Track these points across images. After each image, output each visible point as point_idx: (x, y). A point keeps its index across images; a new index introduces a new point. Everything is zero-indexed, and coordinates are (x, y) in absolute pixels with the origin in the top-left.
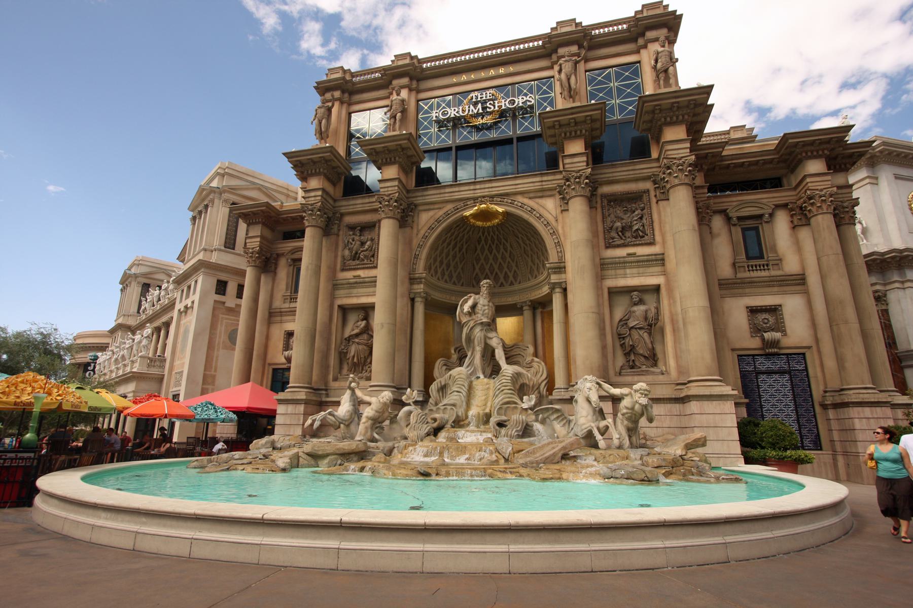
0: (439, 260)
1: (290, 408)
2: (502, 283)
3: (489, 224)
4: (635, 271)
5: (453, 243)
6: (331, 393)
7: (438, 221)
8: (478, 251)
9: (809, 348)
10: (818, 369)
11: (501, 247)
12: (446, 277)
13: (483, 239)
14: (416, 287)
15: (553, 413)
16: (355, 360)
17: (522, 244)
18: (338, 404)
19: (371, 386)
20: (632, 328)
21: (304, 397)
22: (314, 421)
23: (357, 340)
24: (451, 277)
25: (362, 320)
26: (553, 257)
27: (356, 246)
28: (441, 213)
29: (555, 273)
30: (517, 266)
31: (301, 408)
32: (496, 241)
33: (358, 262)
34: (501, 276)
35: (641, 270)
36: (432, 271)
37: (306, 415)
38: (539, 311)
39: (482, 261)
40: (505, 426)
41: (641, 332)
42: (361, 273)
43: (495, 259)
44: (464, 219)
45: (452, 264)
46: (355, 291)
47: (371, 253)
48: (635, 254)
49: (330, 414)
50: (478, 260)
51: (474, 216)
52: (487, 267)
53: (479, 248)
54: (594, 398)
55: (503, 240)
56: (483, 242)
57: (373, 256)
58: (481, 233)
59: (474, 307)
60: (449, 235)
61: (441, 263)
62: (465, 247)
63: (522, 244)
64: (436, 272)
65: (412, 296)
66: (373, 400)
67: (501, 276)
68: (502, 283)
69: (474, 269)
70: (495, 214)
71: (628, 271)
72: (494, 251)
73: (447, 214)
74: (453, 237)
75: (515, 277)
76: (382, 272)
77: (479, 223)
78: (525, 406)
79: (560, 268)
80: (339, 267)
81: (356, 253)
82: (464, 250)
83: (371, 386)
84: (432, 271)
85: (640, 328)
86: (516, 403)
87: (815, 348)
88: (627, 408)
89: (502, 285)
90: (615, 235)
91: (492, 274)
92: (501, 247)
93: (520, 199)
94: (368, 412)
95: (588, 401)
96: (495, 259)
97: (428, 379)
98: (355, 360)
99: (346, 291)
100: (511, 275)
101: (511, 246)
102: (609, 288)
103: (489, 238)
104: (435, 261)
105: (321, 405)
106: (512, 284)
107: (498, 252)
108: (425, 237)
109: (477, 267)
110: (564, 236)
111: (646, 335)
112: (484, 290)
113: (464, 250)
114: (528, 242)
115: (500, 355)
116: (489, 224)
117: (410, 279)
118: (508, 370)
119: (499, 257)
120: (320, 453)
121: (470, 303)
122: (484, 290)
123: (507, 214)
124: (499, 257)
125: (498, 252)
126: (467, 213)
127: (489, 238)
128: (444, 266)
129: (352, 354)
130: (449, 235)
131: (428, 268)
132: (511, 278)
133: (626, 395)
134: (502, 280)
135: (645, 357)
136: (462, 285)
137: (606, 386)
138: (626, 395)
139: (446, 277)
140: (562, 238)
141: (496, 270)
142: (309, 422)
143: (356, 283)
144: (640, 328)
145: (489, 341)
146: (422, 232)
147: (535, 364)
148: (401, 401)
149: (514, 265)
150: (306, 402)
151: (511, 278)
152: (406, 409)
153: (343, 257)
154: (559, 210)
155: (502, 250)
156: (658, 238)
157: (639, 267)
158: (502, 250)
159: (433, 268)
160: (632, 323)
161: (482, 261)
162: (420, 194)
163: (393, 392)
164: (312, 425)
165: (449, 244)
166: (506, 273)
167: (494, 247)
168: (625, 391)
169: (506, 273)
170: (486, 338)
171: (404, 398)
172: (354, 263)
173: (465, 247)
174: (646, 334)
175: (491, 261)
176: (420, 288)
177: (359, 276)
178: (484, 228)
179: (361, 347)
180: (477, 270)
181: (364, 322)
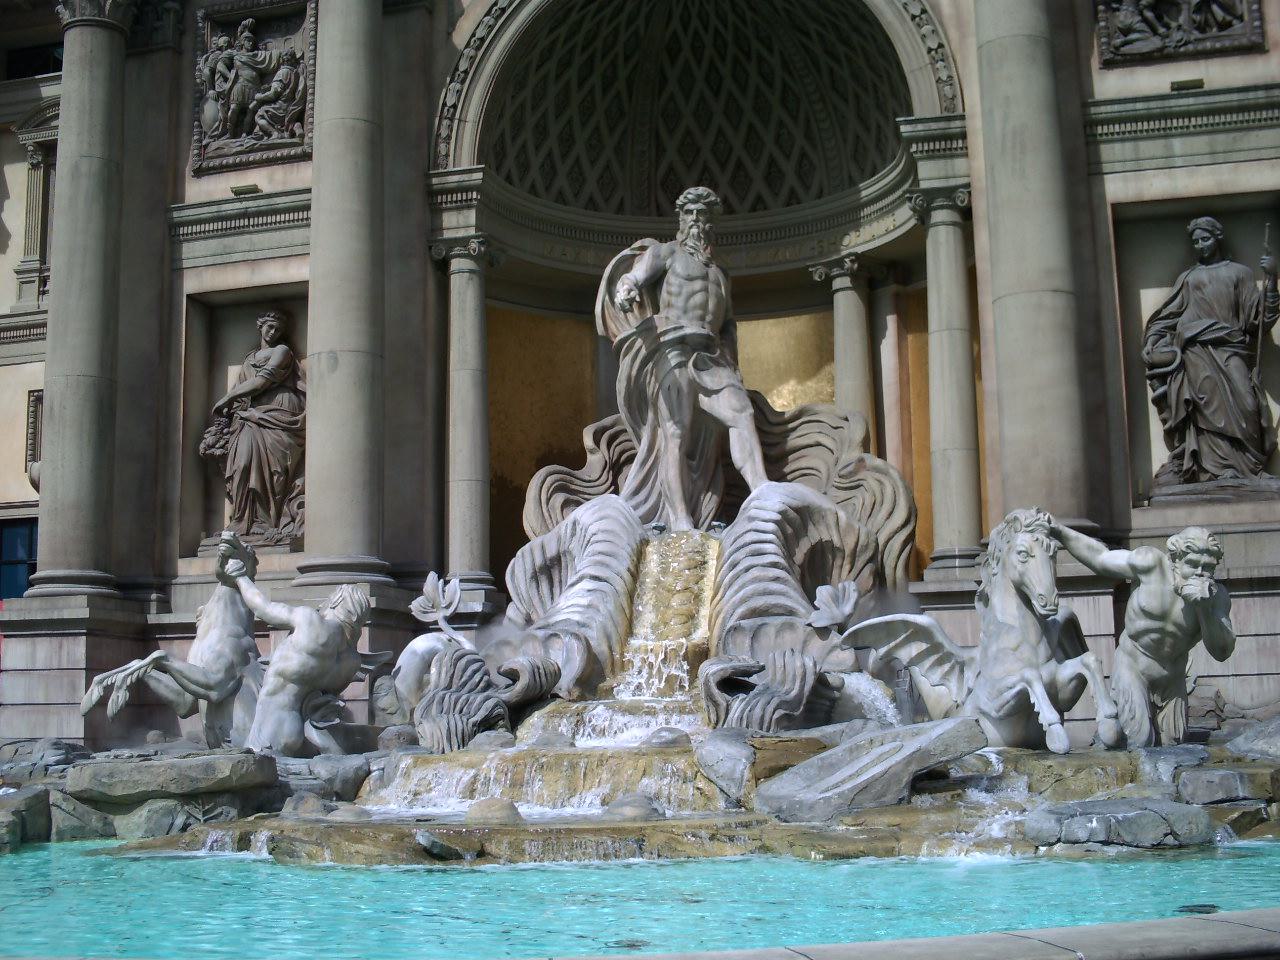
0: (531, 120)
1: (43, 650)
2: (759, 199)
4: (1200, 143)
5: (579, 59)
6: (178, 596)
12: (562, 182)
15: (908, 641)
16: (253, 482)
18: (188, 631)
19: (303, 570)
20: (1191, 342)
21: (84, 613)
22: (108, 690)
23: (255, 413)
24: (577, 177)
25: (273, 343)
26: (925, 99)
29: (932, 155)
30: (808, 136)
31: (77, 649)
33: (247, 141)
34: (757, 173)
35: (1221, 140)
36: (510, 163)
37: (93, 668)
38: (887, 292)
40: (747, 688)
41: (1220, 355)
42: (262, 179)
46: (241, 242)
47: (294, 109)
48: (1199, 84)
49: (160, 666)
54: (1040, 582)
55: (756, 45)
57: (300, 117)
58: (676, 24)
59: (653, 285)
60: (563, 30)
61: (541, 131)
62: (623, 73)
64: (525, 168)
66: (300, 616)
67: (757, 173)
68: (759, 199)
69: (660, 150)
71: (1178, 145)
74: (580, 38)
75: (803, 176)
76: (328, 174)
78: (820, 620)
79: (950, 140)
81: (243, 110)
83: (303, 570)
84: (510, 163)
86: (791, 612)
88: (1147, 614)
89: (759, 204)
90: (1134, 20)
91: (723, 166)
94: (287, 655)
97: (503, 535)
98: (253, 482)
99: (213, 245)
100: (788, 167)
102: (1114, 206)
104: (518, 126)
105: (145, 639)
106: (793, 199)
111: (1235, 367)
112: (689, 225)
114: (841, 49)
118: (767, 498)
120: (119, 792)
121: (640, 271)
122: (689, 225)
128: (552, 143)
129: (241, 462)
130: (563, 30)
131: (490, 151)
132: (791, 180)
133: (1148, 571)
134: (759, 186)
136: (620, 209)
137: (1084, 543)
138: (1148, 571)
139: (562, 182)
140: (953, 34)
142: (96, 692)
143: (245, 214)
144: (1218, 343)
145: (705, 402)
147: (870, 480)
148: (408, 616)
150: (93, 629)
151: (791, 180)
152: (421, 643)
157: (1213, 130)
159: (512, 152)
160: (1189, 326)
163: (375, 589)
164: (103, 702)
165: (565, 64)
166: (772, 162)
167: (726, 70)
169: (772, 162)
171: (416, 606)
173: (623, 73)
174: (1235, 362)
177: (252, 192)
179: (270, 437)
181: (281, 348)
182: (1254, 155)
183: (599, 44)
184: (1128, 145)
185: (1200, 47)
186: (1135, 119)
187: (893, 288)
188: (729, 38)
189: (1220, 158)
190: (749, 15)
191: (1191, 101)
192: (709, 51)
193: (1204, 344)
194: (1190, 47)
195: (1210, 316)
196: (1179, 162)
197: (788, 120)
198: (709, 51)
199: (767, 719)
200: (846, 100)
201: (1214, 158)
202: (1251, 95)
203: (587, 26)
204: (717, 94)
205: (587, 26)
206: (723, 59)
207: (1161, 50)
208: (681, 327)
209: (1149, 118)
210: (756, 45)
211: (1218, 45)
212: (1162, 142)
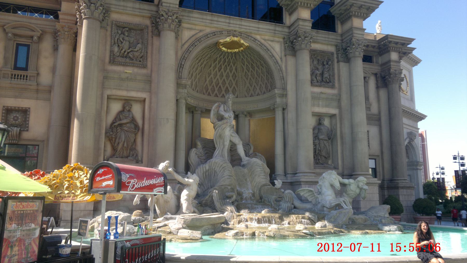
3: (229, 51)
5: (200, 58)
7: (199, 40)
8: (212, 68)
9: (378, 156)
10: (381, 168)
11: (228, 68)
13: (218, 59)
14: (181, 90)
17: (245, 70)
27: (126, 45)
28: (201, 34)
29: (279, 97)
30: (236, 84)
32: (226, 63)
38: (247, 119)
39: (212, 76)
43: (222, 76)
44: (217, 44)
45: (194, 75)
50: (210, 74)
51: (225, 45)
52: (214, 81)
53: (213, 65)
54: (337, 185)
55: (231, 64)
56: (217, 62)
58: (218, 56)
62: (205, 63)
63: (245, 70)
65: (179, 97)
69: (206, 81)
70: (241, 45)
72: (222, 70)
77: (224, 49)
79: (284, 95)
80: (107, 59)
82: (203, 65)
87: (380, 157)
95: (332, 186)
96: (222, 76)
98: (125, 145)
101: (236, 69)
103: (222, 60)
107: (225, 71)
108: (188, 51)
109: (208, 80)
110: (286, 72)
113: (203, 65)
114: (251, 69)
115: (241, 150)
116: (229, 51)
117: (177, 84)
119: (225, 75)
123: (248, 48)
124: (225, 75)
125: (225, 71)
127: (222, 60)
135: (325, 157)
140: (284, 74)
141: (220, 84)
146: (186, 46)
149: (234, 83)
153: (112, 52)
154: (283, 54)
155: (228, 70)
156: (337, 85)
158: (228, 70)
162: (186, 14)
165: (197, 59)
167: (223, 67)
168: (351, 181)
170: (231, 135)
172: (123, 60)
173: (205, 63)
175: (218, 76)
176: (184, 92)
178: (224, 51)
180: (207, 82)
187: (249, 118)
188: (227, 60)
190: (234, 57)
192: (222, 62)
197: (232, 80)
198: (222, 62)
200: (247, 79)
201: (327, 106)
204: (219, 71)
206: (223, 64)
210: (231, 64)
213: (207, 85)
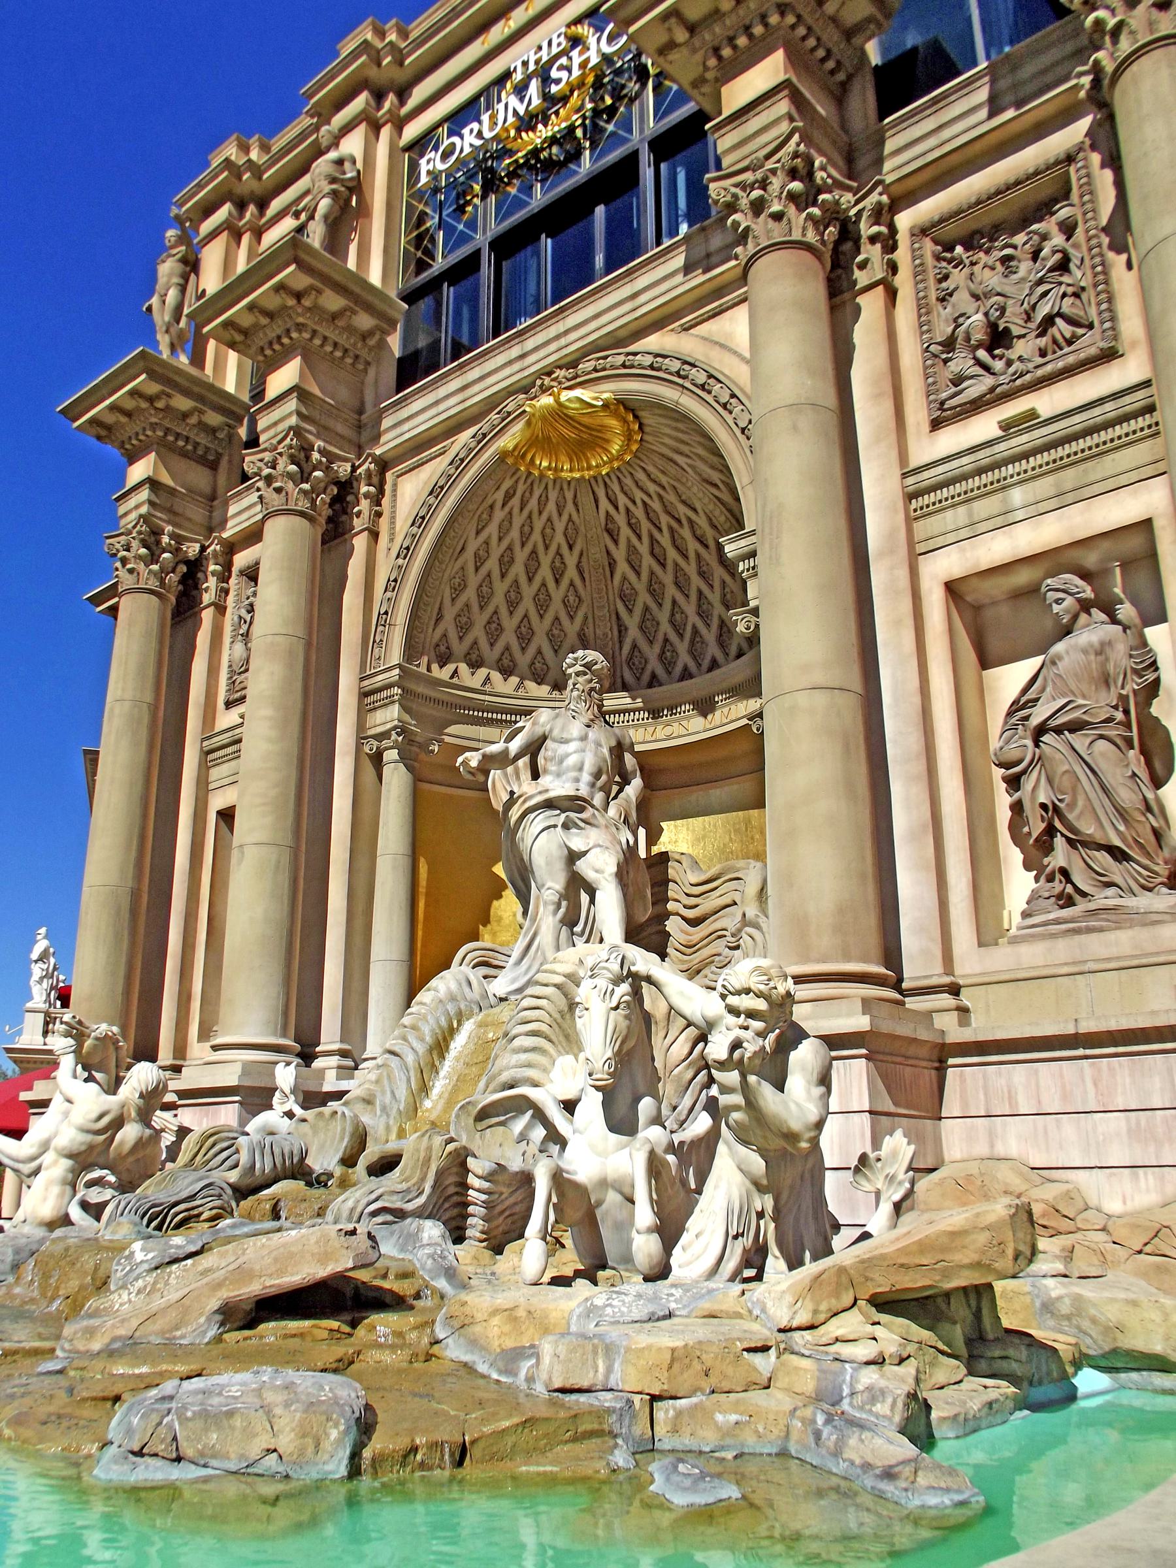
4: (1045, 486)
8: (622, 567)
20: (1040, 731)
50: (627, 598)
53: (620, 554)
58: (604, 504)
71: (1017, 496)
73: (460, 464)
82: (571, 573)
85: (1075, 727)
92: (686, 532)
93: (653, 342)
109: (632, 623)
126: (507, 441)
144: (1075, 727)
157: (1058, 467)
161: (644, 598)
173: (571, 560)
180: (633, 633)
182: (1110, 484)
183: (536, 536)
184: (961, 510)
185: (1040, 373)
186: (964, 477)
189: (1070, 497)
191: (1024, 438)
193: (1058, 731)
194: (1028, 377)
195: (1064, 695)
196: (1020, 515)
199: (359, 1210)
201: (1062, 500)
202: (1097, 411)
203: (518, 521)
205: (518, 521)
207: (992, 390)
208: (547, 791)
209: (980, 472)
211: (1060, 364)
212: (1000, 496)
213: (635, 646)
